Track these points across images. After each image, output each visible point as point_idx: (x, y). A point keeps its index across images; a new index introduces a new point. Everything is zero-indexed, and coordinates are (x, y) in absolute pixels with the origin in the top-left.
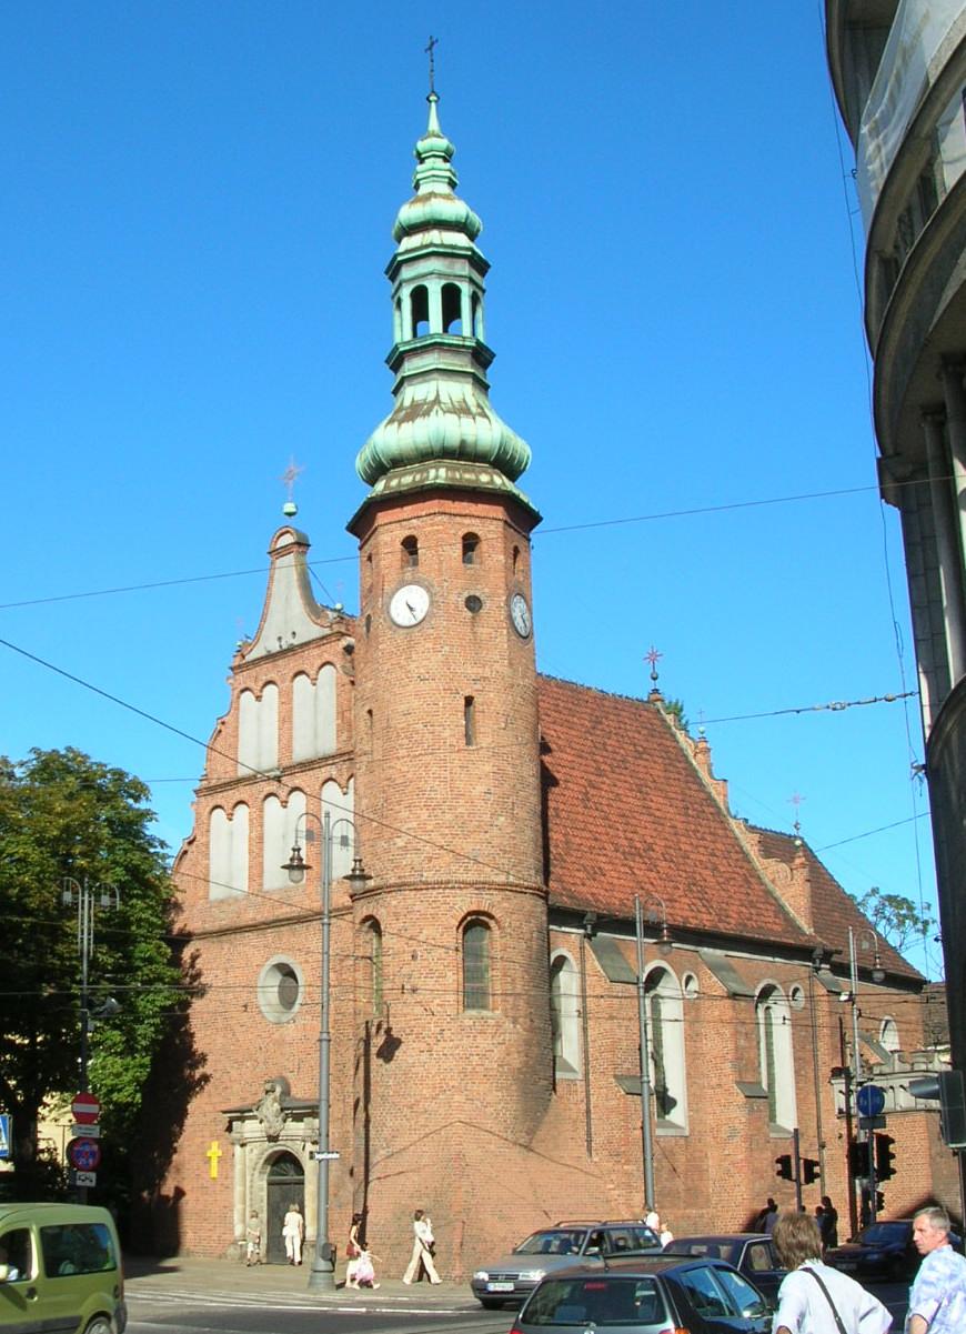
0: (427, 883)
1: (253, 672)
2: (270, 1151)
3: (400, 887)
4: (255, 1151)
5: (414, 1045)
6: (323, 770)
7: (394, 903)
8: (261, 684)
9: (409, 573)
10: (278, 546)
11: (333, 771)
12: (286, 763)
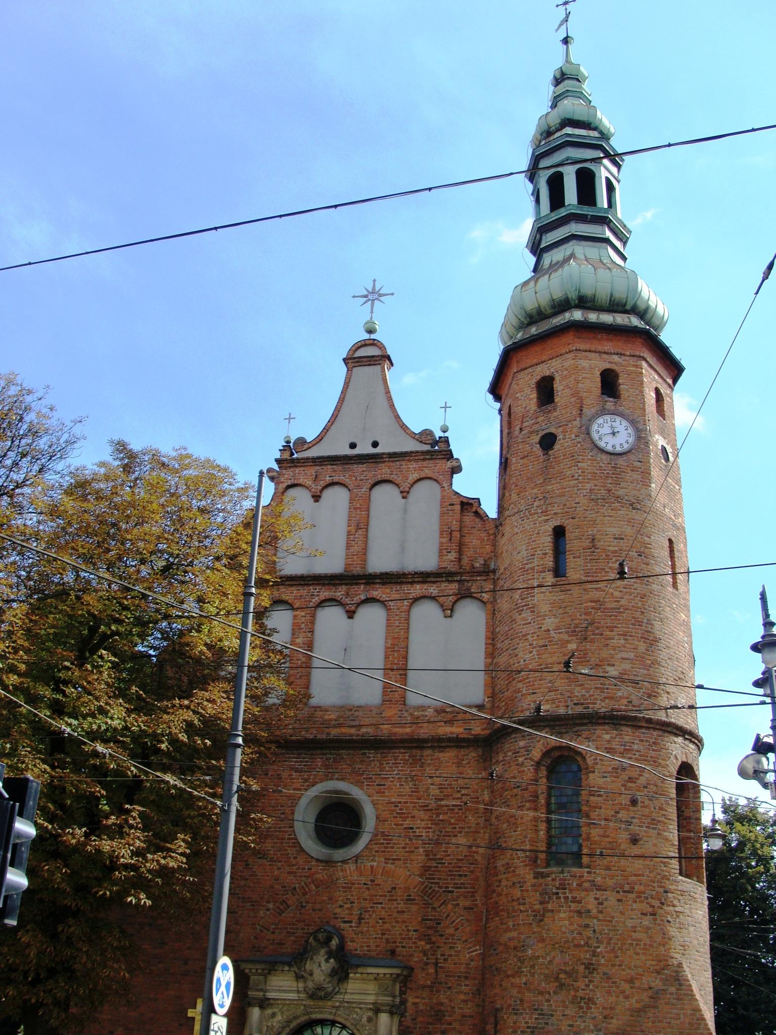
0: (649, 721)
1: (312, 471)
2: (303, 1019)
3: (615, 720)
4: (279, 1017)
5: (634, 905)
6: (418, 587)
7: (607, 737)
8: (322, 483)
9: (610, 403)
10: (357, 354)
11: (433, 590)
12: (357, 570)
